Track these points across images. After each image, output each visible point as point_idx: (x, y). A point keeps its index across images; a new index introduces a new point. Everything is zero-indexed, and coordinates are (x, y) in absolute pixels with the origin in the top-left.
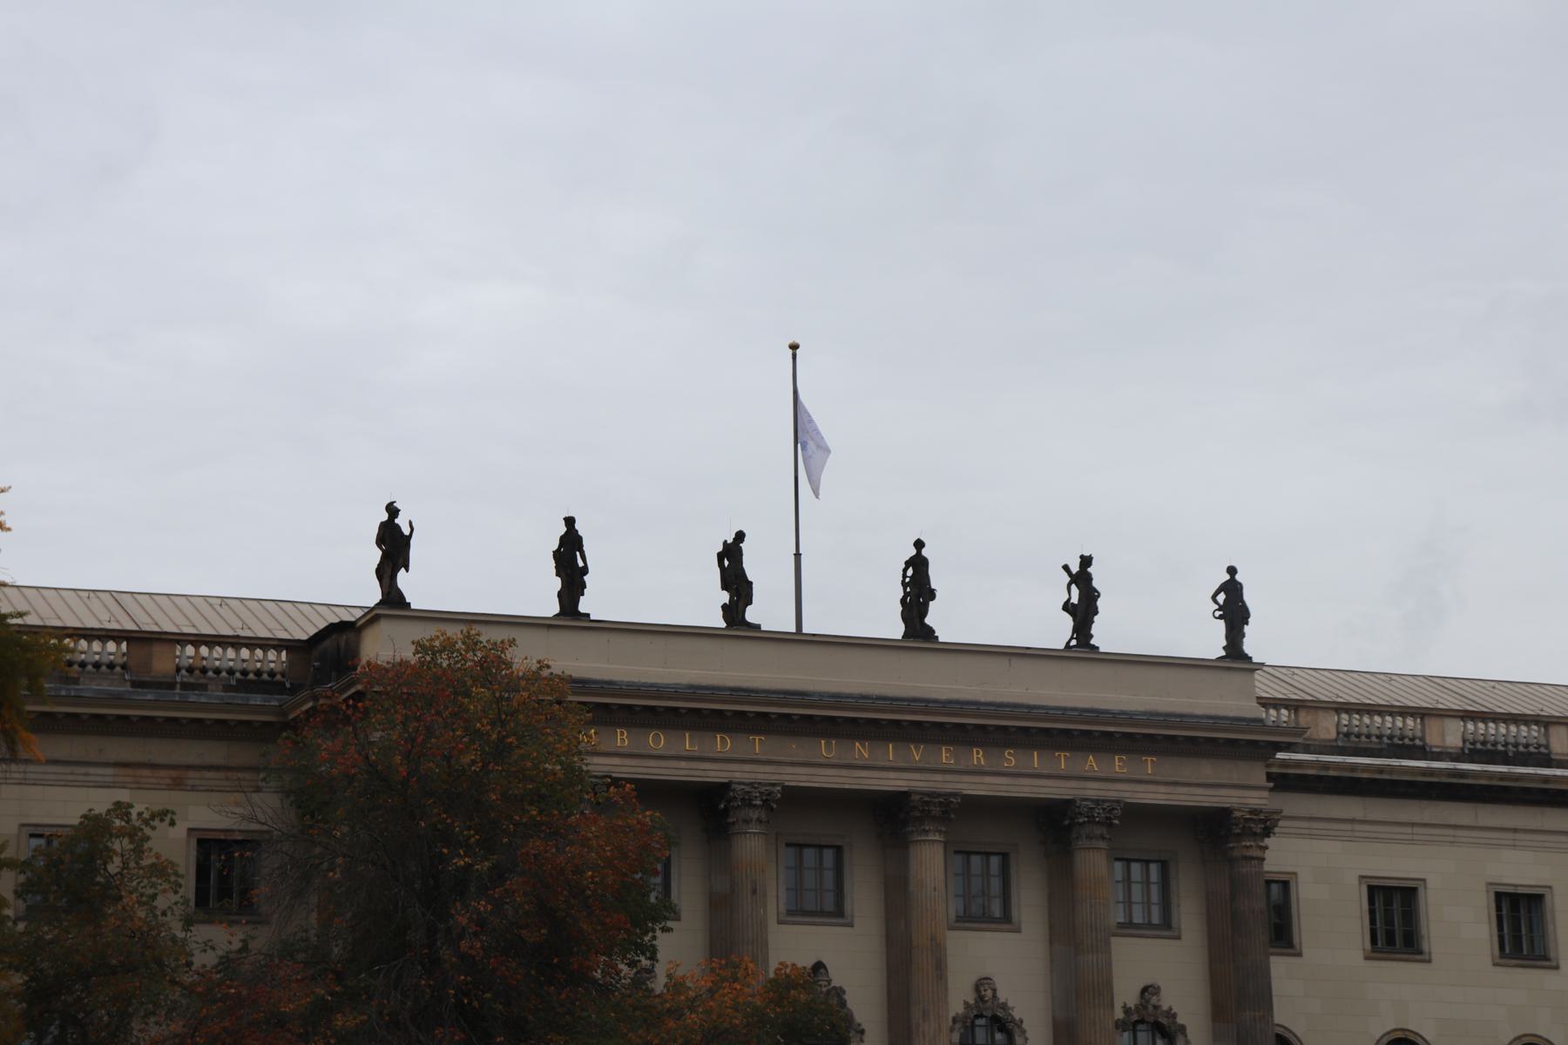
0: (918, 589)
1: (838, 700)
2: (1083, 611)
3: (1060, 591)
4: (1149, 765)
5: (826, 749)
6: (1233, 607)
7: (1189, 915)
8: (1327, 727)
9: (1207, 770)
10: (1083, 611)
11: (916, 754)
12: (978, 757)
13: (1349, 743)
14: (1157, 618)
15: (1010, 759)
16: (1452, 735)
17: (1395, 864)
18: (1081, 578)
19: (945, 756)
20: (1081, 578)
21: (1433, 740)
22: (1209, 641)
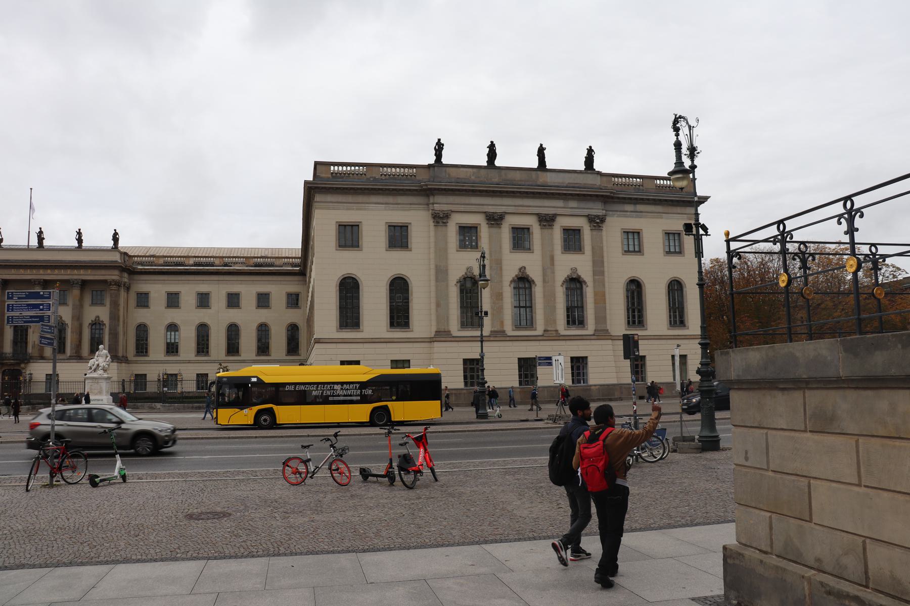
0: (40, 238)
1: (16, 261)
2: (80, 240)
3: (75, 235)
4: (89, 271)
5: (13, 271)
6: (115, 238)
7: (108, 302)
8: (161, 261)
9: (103, 272)
10: (80, 240)
11: (34, 271)
12: (49, 271)
13: (166, 264)
14: (98, 238)
15: (56, 271)
16: (192, 261)
17: (173, 288)
18: (79, 233)
19: (41, 272)
20: (79, 233)
21: (187, 263)
22: (111, 244)
